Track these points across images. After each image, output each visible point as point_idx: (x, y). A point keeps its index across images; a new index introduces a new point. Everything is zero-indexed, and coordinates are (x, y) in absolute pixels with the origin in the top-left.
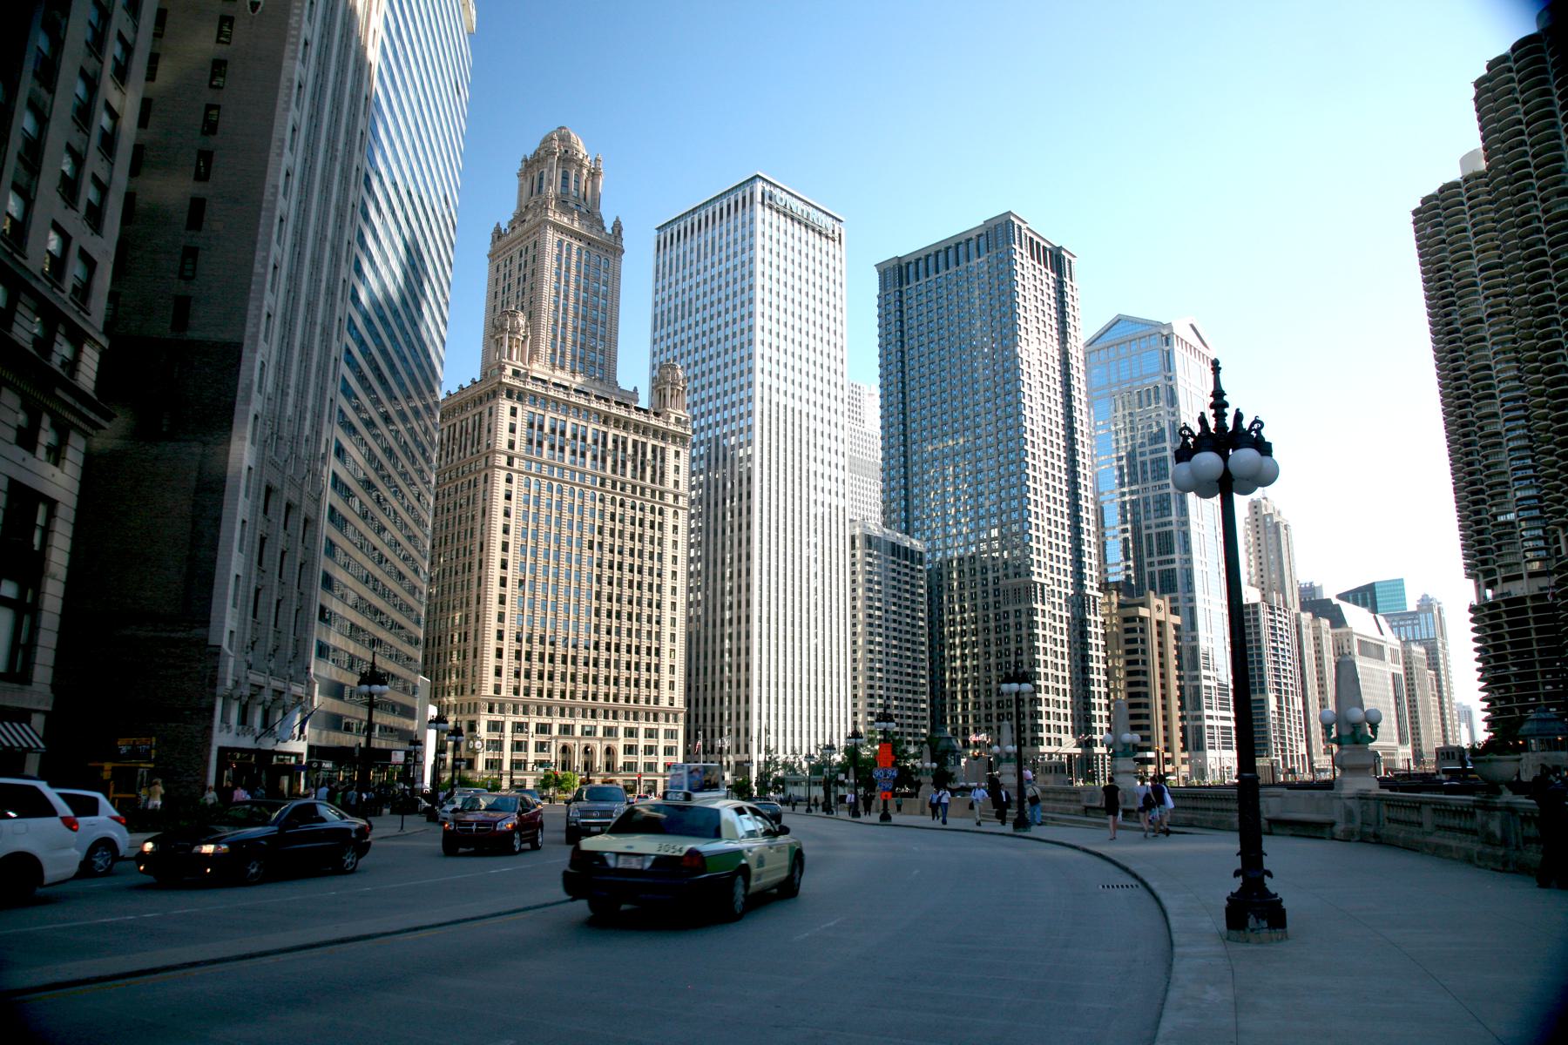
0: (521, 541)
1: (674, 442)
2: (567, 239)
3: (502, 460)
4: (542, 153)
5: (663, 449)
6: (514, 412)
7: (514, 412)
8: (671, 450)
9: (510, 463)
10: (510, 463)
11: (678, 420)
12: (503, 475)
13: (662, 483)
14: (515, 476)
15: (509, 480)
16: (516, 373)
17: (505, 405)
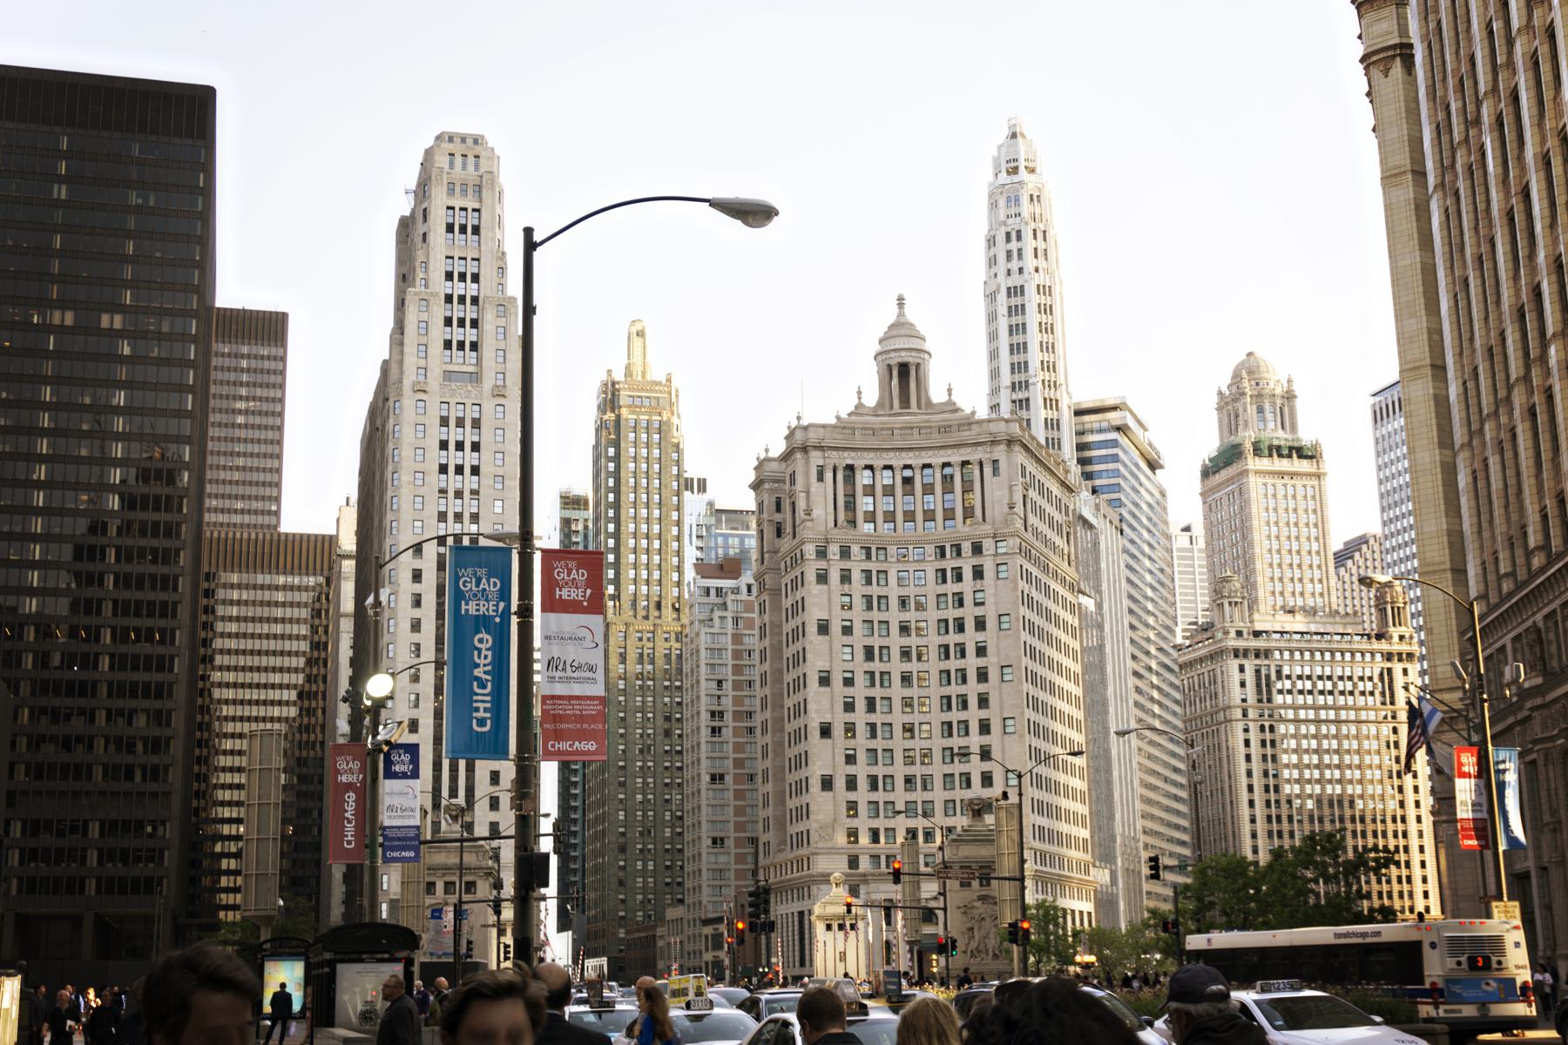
0: (1264, 781)
1: (1400, 660)
2: (1270, 481)
3: (1238, 713)
4: (1234, 389)
5: (1389, 670)
6: (1242, 669)
7: (1242, 669)
8: (1398, 668)
9: (1245, 715)
10: (1245, 715)
11: (1401, 638)
12: (1240, 726)
13: (1392, 703)
14: (1251, 724)
15: (1246, 730)
16: (1239, 634)
17: (1234, 664)
